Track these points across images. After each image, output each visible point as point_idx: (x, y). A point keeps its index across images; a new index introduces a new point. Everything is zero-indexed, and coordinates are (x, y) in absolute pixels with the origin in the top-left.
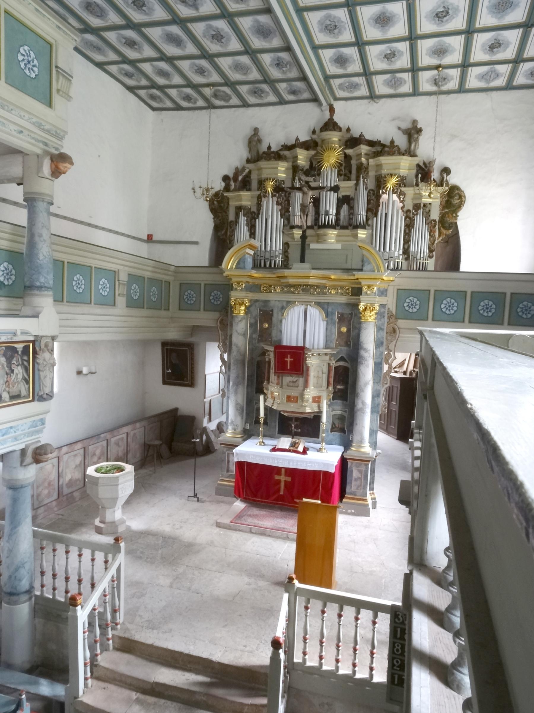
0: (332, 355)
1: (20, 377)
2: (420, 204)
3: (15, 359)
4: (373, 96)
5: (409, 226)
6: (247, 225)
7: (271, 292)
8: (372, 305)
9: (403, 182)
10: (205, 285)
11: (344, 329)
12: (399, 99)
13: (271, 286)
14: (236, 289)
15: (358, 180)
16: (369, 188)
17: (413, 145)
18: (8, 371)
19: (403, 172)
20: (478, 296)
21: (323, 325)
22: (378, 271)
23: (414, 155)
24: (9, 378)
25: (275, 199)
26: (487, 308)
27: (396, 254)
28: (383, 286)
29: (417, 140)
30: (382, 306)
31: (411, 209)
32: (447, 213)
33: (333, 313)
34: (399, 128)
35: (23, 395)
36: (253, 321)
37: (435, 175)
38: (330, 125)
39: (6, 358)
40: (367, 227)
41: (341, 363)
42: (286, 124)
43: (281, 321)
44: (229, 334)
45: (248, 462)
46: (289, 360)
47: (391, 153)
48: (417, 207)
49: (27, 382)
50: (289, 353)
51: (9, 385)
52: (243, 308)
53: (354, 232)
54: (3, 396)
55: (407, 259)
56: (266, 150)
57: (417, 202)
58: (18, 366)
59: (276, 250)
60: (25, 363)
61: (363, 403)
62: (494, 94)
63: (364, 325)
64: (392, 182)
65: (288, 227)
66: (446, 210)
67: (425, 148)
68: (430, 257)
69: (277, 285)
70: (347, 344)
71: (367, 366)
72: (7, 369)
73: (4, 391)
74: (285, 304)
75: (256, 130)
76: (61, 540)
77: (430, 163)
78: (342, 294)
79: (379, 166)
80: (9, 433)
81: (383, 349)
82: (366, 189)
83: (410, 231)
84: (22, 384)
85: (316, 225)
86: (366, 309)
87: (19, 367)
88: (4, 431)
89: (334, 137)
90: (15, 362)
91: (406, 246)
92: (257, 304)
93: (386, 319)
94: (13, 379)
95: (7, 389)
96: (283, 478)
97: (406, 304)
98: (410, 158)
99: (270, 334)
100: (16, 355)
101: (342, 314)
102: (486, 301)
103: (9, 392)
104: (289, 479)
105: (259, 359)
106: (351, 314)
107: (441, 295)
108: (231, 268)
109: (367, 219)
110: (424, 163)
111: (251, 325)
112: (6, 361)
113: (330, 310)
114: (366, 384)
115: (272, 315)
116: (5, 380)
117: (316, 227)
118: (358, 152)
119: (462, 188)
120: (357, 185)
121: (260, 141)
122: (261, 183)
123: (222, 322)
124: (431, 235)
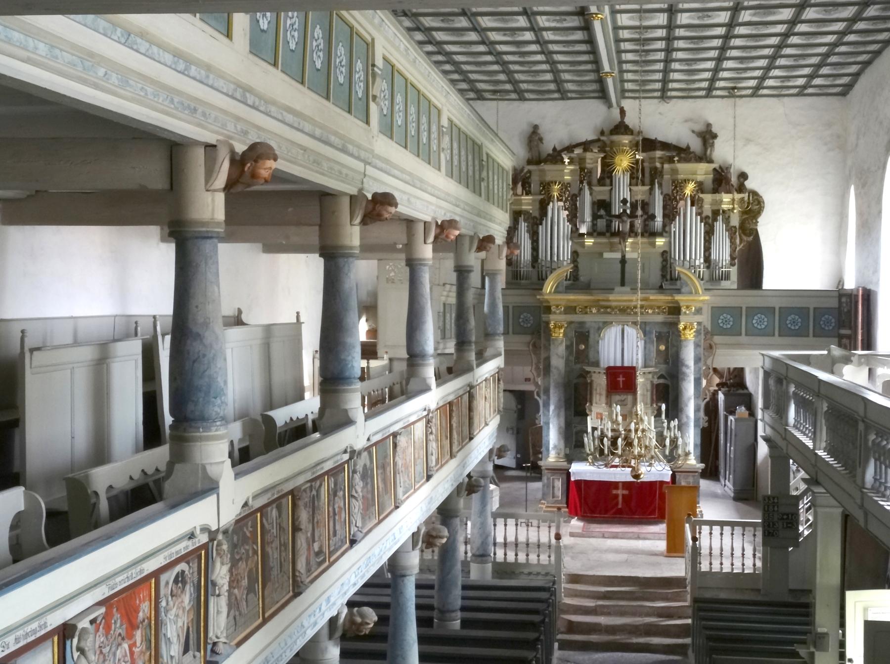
0: (655, 373)
2: (719, 211)
4: (664, 95)
5: (709, 233)
6: (528, 231)
7: (586, 313)
8: (692, 324)
9: (701, 187)
10: (514, 307)
11: (662, 348)
12: (690, 100)
13: (586, 307)
14: (555, 313)
15: (652, 184)
16: (665, 192)
17: (709, 151)
19: (700, 178)
20: (785, 311)
21: (641, 344)
22: (696, 293)
23: (711, 161)
25: (561, 204)
26: (794, 322)
27: (697, 263)
28: (699, 305)
29: (712, 145)
30: (699, 324)
31: (710, 215)
32: (747, 219)
33: (651, 333)
34: (693, 132)
36: (569, 343)
37: (734, 180)
38: (621, 128)
40: (664, 234)
41: (662, 381)
42: (570, 121)
43: (598, 342)
44: (543, 355)
45: (586, 482)
46: (621, 379)
47: (687, 160)
48: (716, 213)
50: (620, 373)
52: (562, 331)
53: (651, 240)
55: (708, 267)
56: (551, 152)
57: (715, 208)
59: (564, 260)
61: (688, 417)
62: (786, 99)
63: (684, 343)
64: (689, 189)
65: (576, 235)
66: (746, 216)
67: (722, 152)
68: (732, 265)
69: (593, 307)
70: (666, 362)
71: (689, 382)
74: (601, 325)
75: (536, 127)
76: (511, 516)
77: (727, 168)
78: (659, 314)
79: (675, 172)
81: (701, 364)
82: (662, 193)
83: (710, 238)
85: (607, 231)
86: (685, 328)
89: (626, 139)
91: (707, 254)
92: (573, 326)
93: (703, 337)
96: (620, 492)
97: (720, 321)
98: (706, 164)
99: (587, 356)
101: (660, 333)
102: (793, 316)
104: (626, 492)
105: (575, 381)
106: (669, 332)
107: (752, 311)
108: (550, 292)
109: (664, 226)
110: (720, 167)
111: (567, 347)
113: (648, 329)
114: (689, 399)
115: (588, 336)
117: (608, 234)
118: (653, 156)
119: (761, 193)
120: (652, 190)
121: (541, 140)
122: (546, 186)
123: (534, 345)
124: (732, 242)
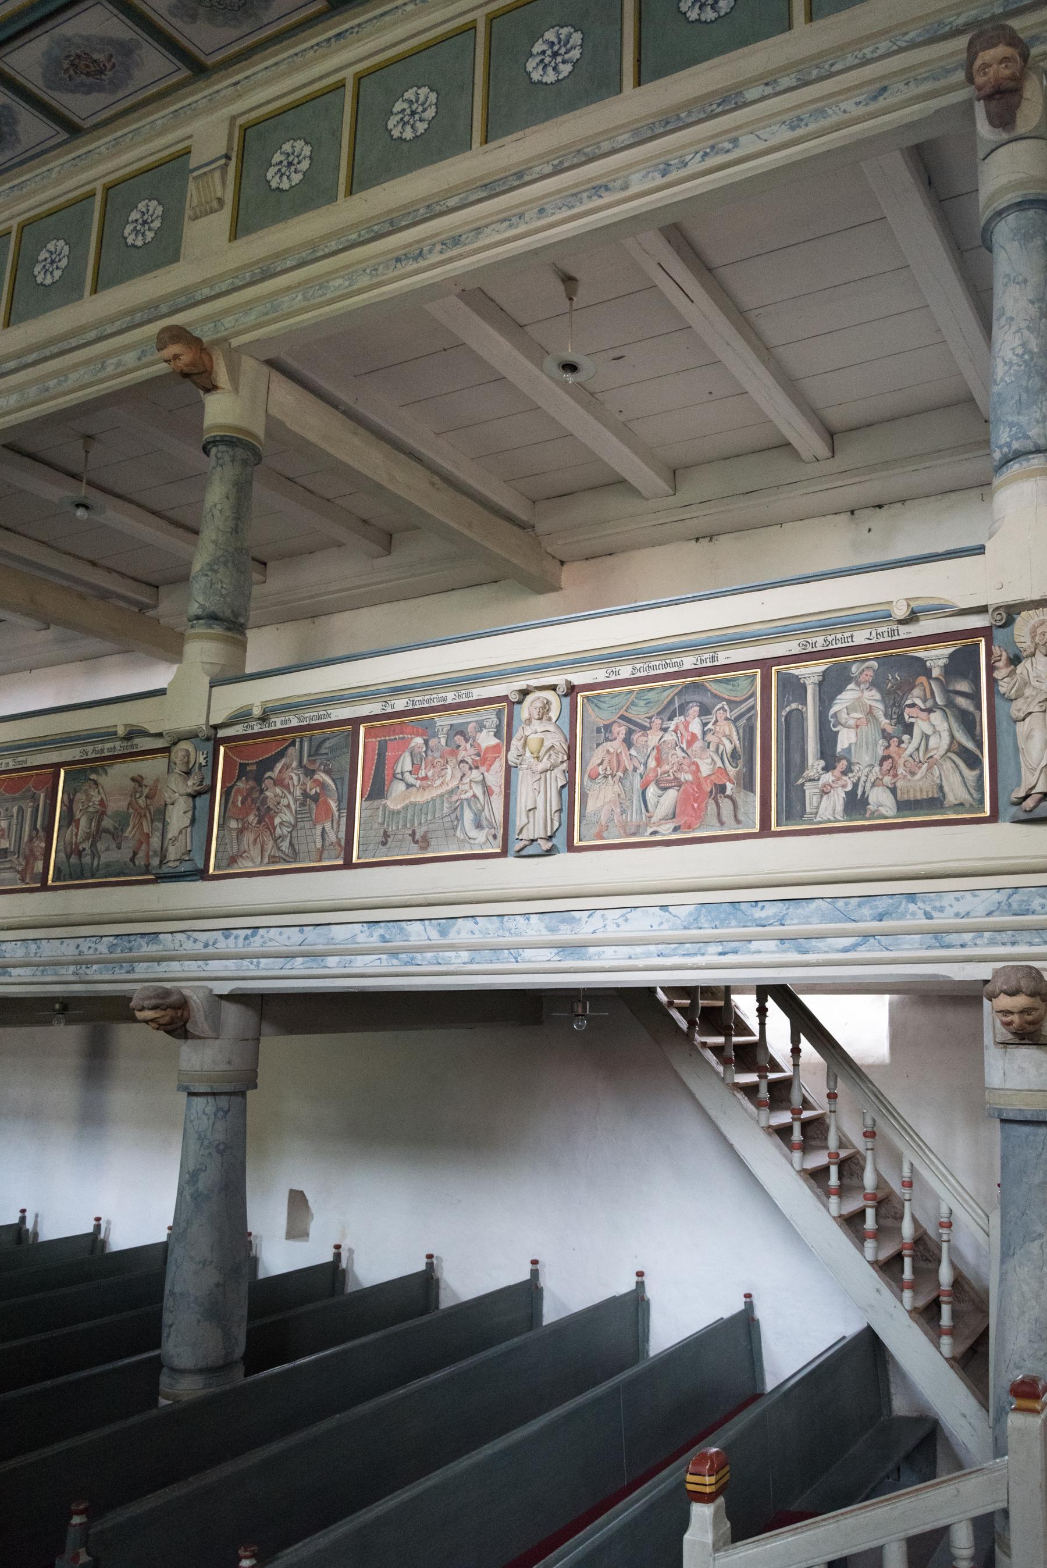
1: (940, 743)
3: (917, 692)
18: (890, 729)
24: (893, 749)
35: (951, 799)
39: (880, 690)
49: (973, 761)
51: (894, 767)
54: (870, 800)
58: (930, 711)
60: (962, 702)
72: (884, 722)
73: (873, 785)
80: (903, 916)
84: (948, 765)
87: (936, 717)
88: (882, 904)
90: (918, 702)
94: (911, 748)
95: (888, 780)
100: (922, 679)
103: (893, 791)
112: (883, 700)
116: (881, 752)
